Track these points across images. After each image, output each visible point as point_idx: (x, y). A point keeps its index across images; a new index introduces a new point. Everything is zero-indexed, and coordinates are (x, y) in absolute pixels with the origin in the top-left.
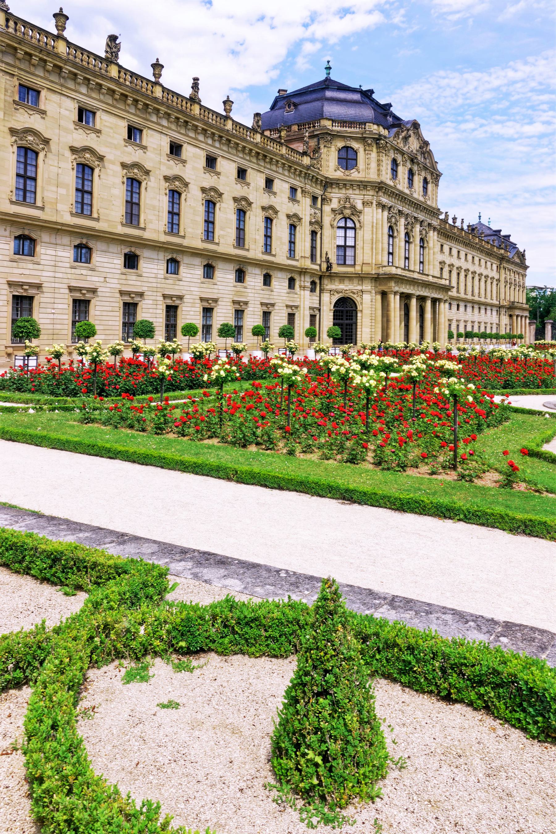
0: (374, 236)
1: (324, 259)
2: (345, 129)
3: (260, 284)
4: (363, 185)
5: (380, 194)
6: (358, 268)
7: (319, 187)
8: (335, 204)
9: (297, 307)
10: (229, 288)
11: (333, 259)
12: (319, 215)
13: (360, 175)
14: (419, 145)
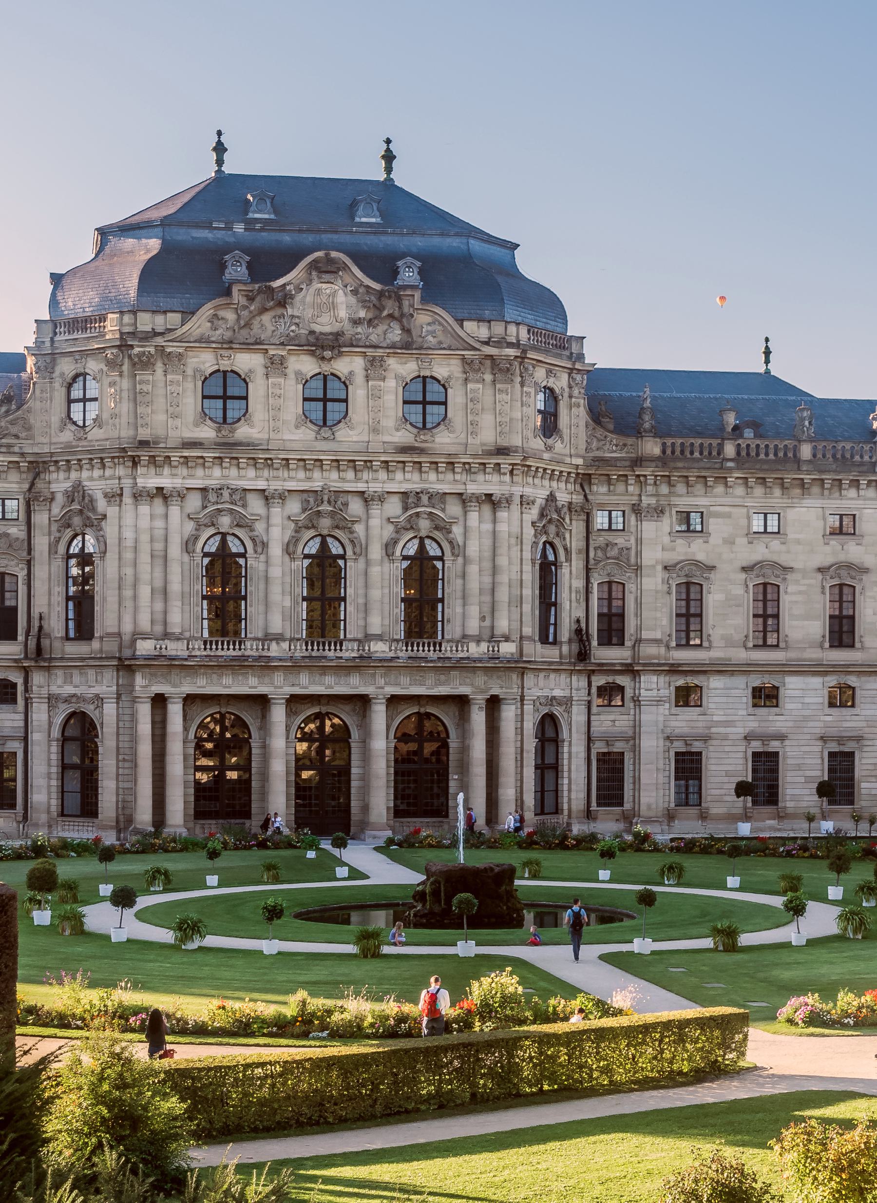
0: (129, 571)
1: (35, 630)
2: (75, 336)
5: (140, 470)
6: (95, 644)
7: (14, 476)
8: (56, 510)
11: (56, 626)
12: (23, 535)
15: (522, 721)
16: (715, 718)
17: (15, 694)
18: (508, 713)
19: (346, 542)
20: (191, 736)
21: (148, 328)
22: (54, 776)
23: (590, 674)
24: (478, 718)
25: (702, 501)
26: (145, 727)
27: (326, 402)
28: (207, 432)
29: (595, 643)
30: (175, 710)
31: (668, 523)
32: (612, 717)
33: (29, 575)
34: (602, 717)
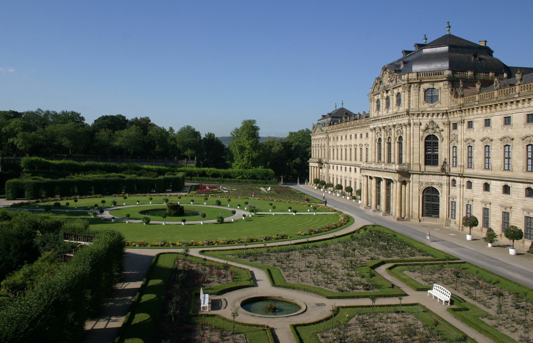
16: (475, 194)
23: (449, 176)
25: (471, 117)
31: (466, 124)
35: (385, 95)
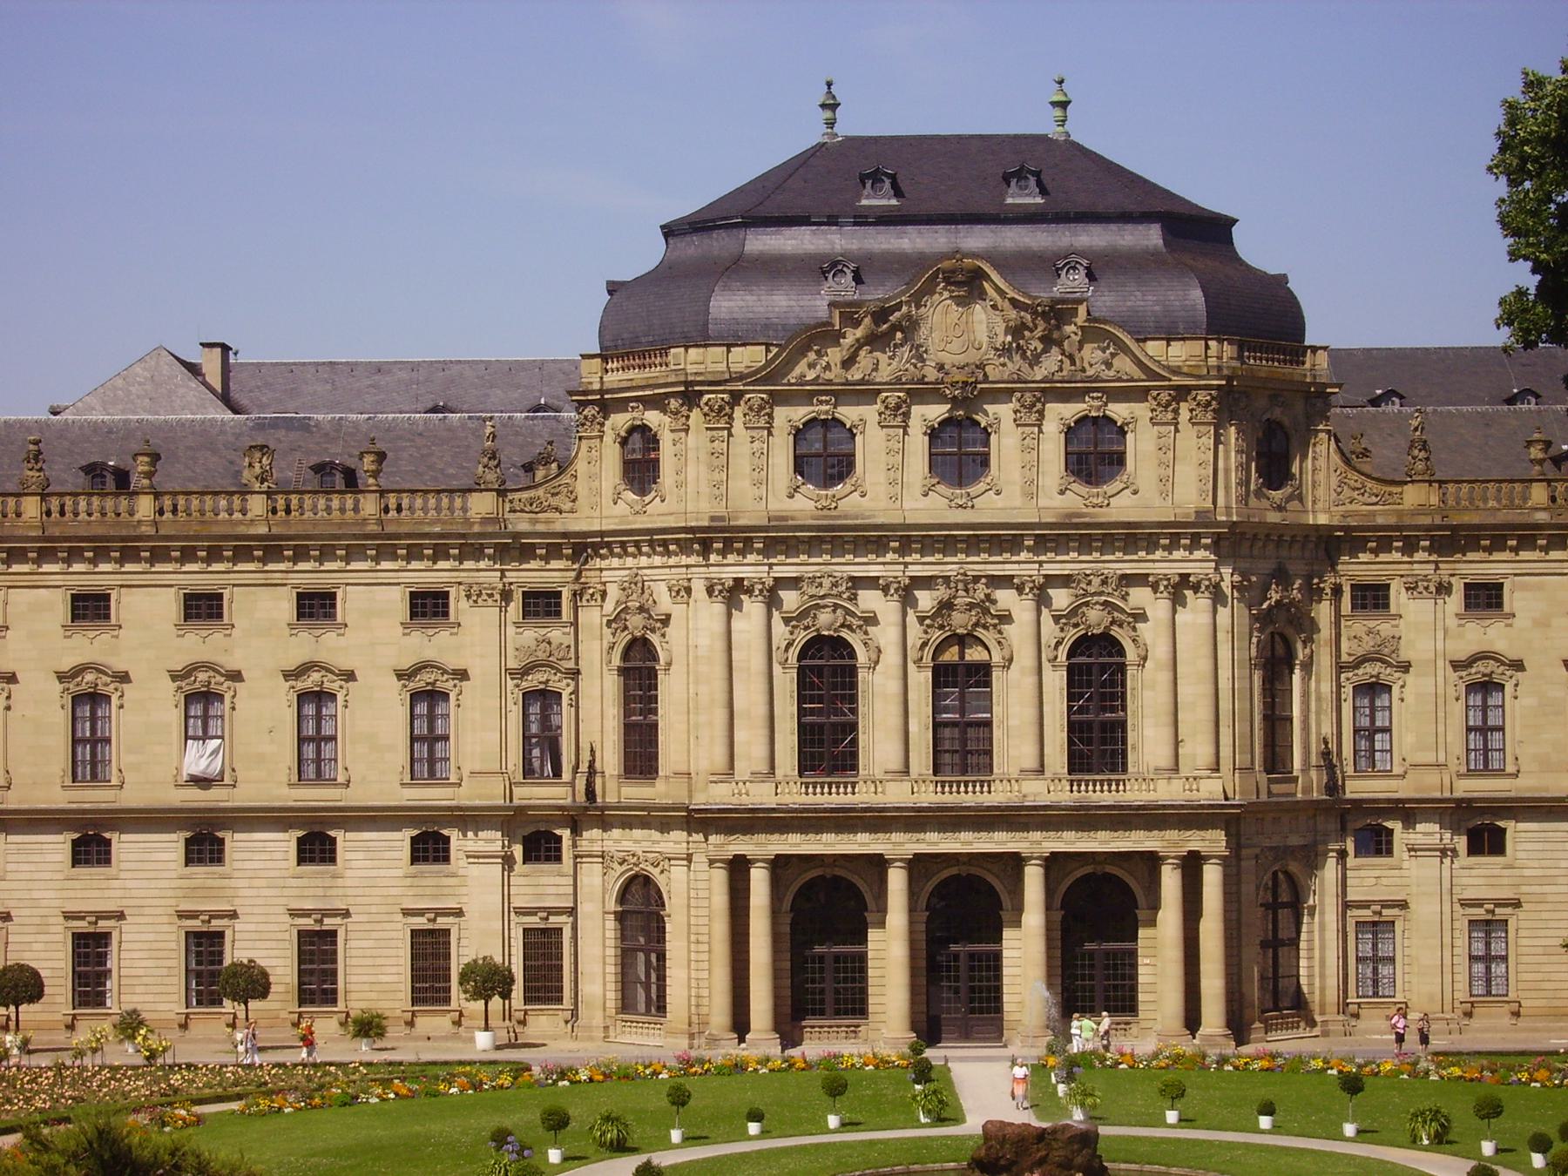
1: (584, 767)
2: (631, 374)
3: (284, 864)
4: (659, 541)
5: (713, 558)
8: (609, 606)
9: (459, 913)
10: (165, 884)
13: (664, 508)
14: (1000, 328)
15: (1239, 883)
16: (1527, 872)
17: (559, 850)
18: (1212, 876)
19: (992, 644)
20: (787, 905)
21: (722, 367)
22: (612, 960)
24: (1170, 882)
26: (720, 899)
27: (959, 454)
28: (805, 504)
29: (1350, 770)
30: (759, 880)
31: (1455, 601)
32: (1377, 873)
33: (576, 692)
34: (1362, 873)
35: (937, 412)
